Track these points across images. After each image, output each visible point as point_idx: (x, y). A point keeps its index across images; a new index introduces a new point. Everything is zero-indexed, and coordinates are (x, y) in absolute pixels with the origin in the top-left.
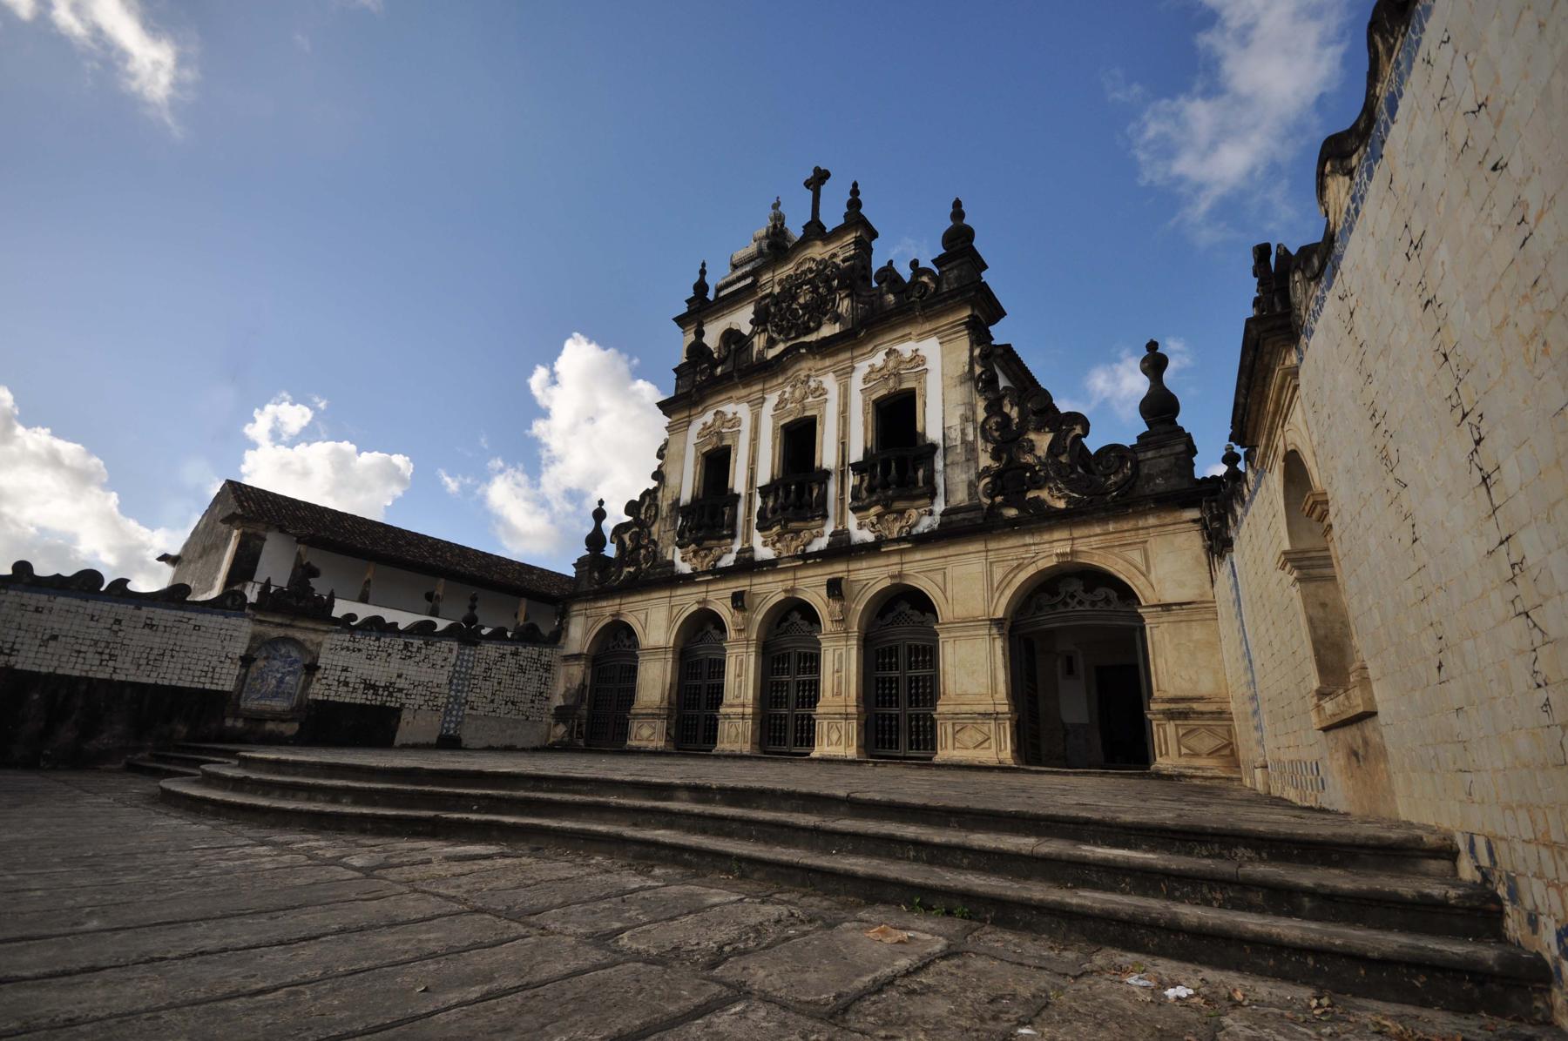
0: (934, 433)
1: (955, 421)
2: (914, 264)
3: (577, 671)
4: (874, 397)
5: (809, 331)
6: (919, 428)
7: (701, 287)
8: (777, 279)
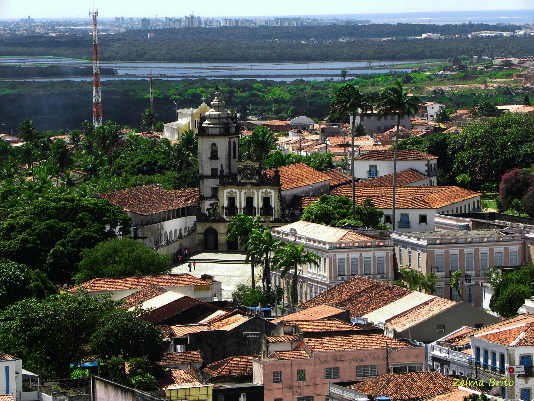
0: (273, 206)
1: (276, 205)
3: (202, 237)
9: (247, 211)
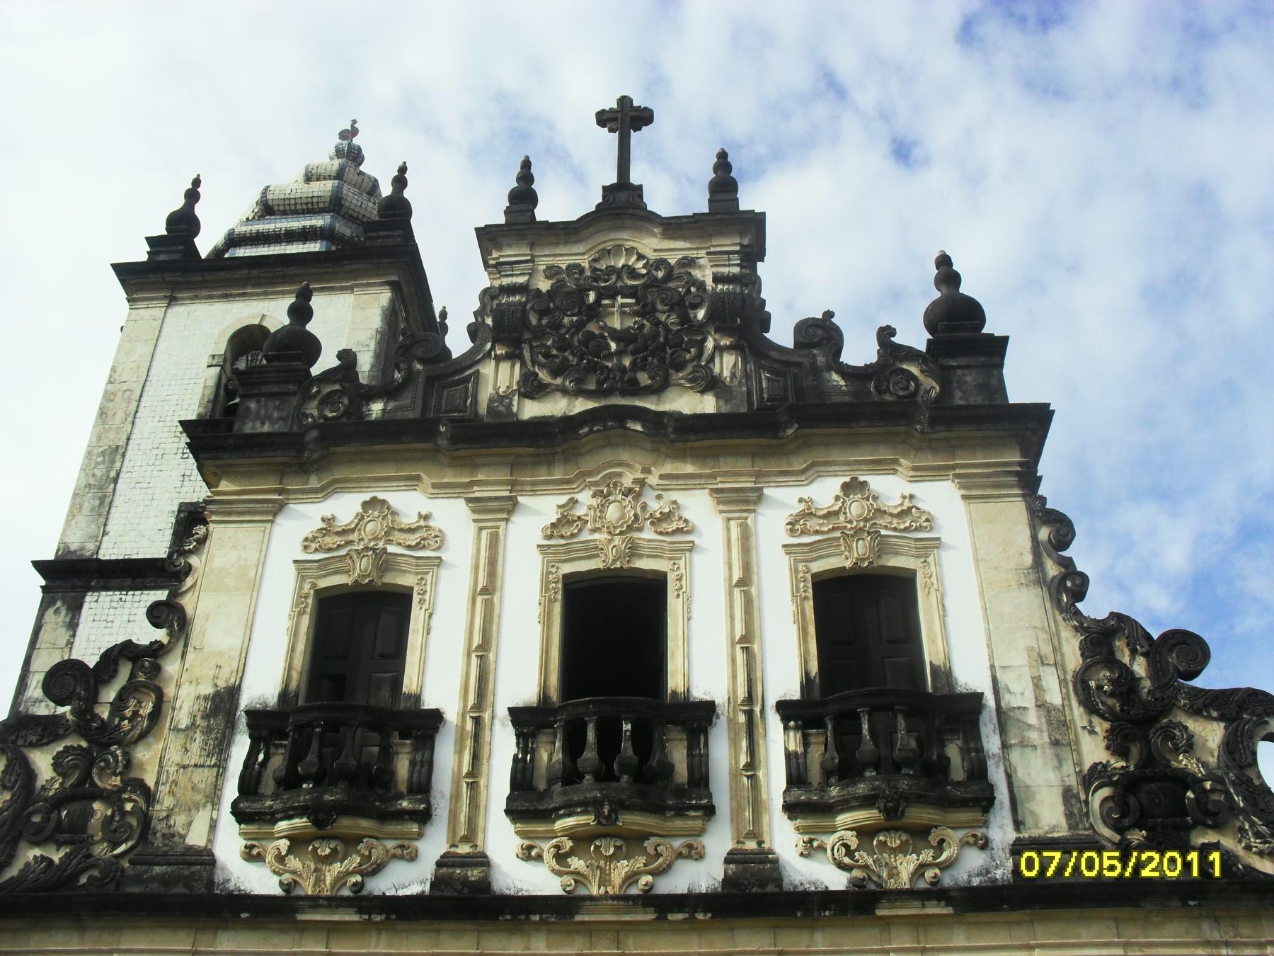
0: (971, 675)
2: (885, 334)
4: (817, 567)
5: (634, 389)
6: (931, 653)
7: (184, 223)
8: (542, 264)
9: (574, 746)
